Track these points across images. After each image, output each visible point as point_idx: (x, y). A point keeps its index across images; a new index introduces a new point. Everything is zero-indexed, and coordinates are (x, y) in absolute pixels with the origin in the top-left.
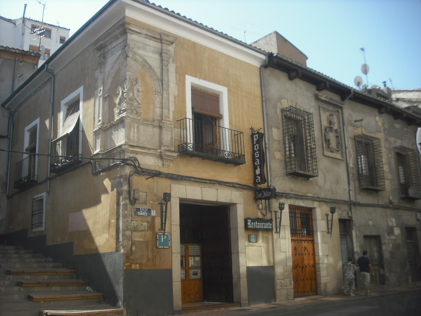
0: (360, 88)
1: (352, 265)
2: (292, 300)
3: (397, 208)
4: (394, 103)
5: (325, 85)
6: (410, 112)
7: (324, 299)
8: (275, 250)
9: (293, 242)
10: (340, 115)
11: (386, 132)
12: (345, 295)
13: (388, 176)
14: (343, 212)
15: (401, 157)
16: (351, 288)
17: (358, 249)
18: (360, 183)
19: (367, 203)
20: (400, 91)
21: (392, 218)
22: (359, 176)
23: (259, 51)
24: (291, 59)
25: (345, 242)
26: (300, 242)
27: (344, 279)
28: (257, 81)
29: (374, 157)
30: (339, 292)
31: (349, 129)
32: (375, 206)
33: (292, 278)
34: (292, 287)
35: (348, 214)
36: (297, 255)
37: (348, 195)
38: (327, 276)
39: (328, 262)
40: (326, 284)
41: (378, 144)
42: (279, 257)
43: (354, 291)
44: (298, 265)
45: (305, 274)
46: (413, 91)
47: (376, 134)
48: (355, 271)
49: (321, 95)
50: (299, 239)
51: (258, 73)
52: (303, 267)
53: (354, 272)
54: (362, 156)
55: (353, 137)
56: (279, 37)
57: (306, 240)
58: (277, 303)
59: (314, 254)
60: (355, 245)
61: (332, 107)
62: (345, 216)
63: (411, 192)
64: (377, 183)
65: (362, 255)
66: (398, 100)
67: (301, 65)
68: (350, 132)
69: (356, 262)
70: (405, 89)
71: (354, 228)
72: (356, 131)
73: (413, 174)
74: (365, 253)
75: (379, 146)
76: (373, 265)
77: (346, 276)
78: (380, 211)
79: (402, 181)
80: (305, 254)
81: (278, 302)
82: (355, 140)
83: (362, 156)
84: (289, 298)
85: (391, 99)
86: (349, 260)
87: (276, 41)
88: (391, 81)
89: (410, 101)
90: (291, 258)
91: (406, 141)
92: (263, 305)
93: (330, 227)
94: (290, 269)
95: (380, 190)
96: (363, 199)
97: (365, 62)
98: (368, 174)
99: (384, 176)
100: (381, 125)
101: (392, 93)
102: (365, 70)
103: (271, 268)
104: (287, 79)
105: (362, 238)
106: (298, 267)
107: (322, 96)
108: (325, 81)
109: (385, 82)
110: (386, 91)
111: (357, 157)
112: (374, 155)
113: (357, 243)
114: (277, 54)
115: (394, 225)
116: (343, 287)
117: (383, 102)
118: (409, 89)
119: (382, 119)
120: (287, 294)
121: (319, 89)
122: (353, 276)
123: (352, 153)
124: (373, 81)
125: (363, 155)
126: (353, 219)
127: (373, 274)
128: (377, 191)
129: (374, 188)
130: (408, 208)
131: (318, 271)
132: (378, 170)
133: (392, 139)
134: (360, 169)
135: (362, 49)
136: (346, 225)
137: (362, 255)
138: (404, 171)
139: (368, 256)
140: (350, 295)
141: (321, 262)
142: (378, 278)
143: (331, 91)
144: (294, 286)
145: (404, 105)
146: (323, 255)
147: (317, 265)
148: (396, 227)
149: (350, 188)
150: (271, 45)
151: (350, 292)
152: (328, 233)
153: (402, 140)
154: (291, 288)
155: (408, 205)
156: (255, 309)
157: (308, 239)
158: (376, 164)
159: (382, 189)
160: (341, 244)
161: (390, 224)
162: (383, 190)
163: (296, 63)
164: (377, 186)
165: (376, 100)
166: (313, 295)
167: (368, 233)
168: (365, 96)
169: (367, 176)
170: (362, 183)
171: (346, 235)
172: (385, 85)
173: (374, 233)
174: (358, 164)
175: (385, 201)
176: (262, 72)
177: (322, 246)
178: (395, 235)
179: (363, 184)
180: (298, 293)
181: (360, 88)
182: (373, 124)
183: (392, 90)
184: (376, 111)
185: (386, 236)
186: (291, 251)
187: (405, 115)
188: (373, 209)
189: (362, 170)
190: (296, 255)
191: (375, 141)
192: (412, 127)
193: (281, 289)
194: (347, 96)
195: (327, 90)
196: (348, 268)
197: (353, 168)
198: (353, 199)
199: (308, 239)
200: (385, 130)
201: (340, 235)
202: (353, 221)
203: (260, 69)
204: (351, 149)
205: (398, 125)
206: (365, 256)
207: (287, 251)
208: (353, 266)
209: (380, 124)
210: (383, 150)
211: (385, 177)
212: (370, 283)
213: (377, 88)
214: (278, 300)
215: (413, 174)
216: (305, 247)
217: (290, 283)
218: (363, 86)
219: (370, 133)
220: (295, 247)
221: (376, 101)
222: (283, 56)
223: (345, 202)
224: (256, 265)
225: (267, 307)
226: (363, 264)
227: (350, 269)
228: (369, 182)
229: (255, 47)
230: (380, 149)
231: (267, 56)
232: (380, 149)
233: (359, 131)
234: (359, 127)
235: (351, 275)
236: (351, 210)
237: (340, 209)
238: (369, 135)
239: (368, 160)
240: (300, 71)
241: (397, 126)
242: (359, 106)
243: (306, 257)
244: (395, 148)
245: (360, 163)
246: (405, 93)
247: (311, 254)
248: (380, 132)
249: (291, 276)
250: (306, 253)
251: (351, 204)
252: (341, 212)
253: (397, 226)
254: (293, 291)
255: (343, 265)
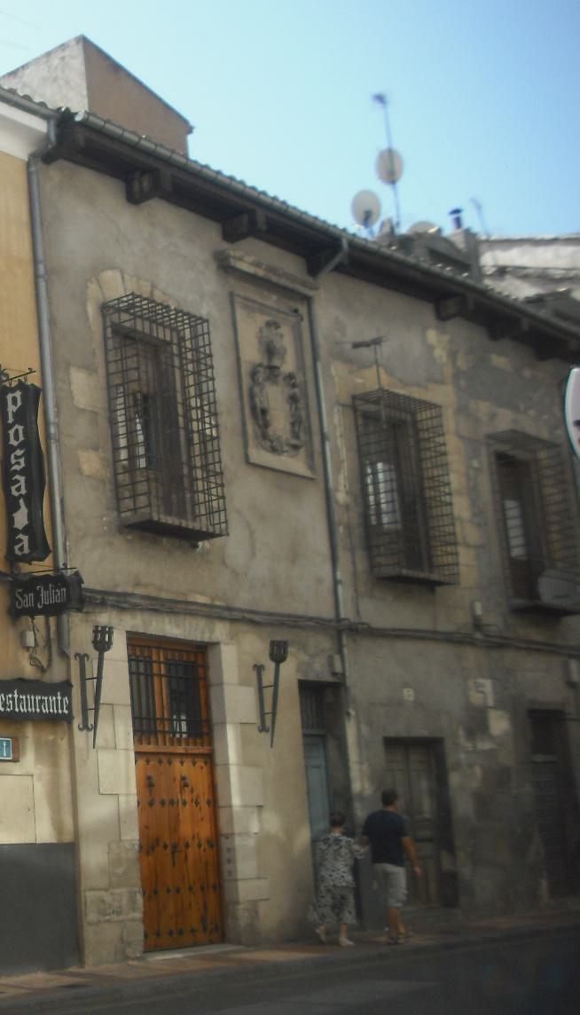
0: (371, 233)
1: (345, 839)
2: (137, 958)
3: (498, 644)
4: (488, 282)
5: (253, 222)
6: (543, 313)
7: (247, 956)
8: (80, 789)
9: (142, 762)
10: (305, 324)
11: (463, 383)
12: (321, 943)
13: (468, 532)
14: (313, 656)
15: (513, 467)
16: (340, 920)
17: (367, 785)
18: (370, 558)
19: (397, 626)
20: (508, 243)
21: (483, 677)
22: (370, 535)
23: (25, 104)
24: (134, 133)
25: (320, 761)
26: (164, 759)
27: (317, 888)
28: (19, 208)
29: (420, 469)
30: (300, 933)
31: (333, 372)
32: (422, 638)
33: (139, 883)
34: (138, 915)
35: (331, 665)
36: (157, 805)
37: (330, 601)
38: (258, 878)
39: (262, 829)
40: (254, 904)
41: (435, 422)
42: (95, 811)
43: (351, 929)
44: (157, 841)
45: (183, 871)
46: (554, 241)
47: (426, 388)
48: (356, 861)
49: (238, 254)
50: (162, 749)
51: (20, 179)
52: (175, 848)
53: (351, 862)
54: (380, 466)
55: (348, 401)
56: (94, 56)
57: (187, 755)
58: (87, 969)
59: (214, 801)
60: (356, 770)
61: (275, 297)
62: (319, 671)
63: (550, 589)
64: (430, 557)
65: (379, 807)
66: (502, 271)
67: (168, 154)
68: (337, 383)
69: (359, 830)
70: (525, 235)
71: (352, 712)
72: (359, 381)
73: (555, 528)
74: (388, 798)
75: (438, 430)
76: (417, 840)
77: (323, 879)
78: (440, 653)
79: (517, 552)
80: (184, 803)
81: (89, 967)
82: (355, 410)
83: (380, 466)
84: (129, 951)
85: (480, 269)
86: (334, 823)
87: (83, 69)
88: (479, 207)
89: (543, 276)
90: (136, 815)
91: (531, 412)
92: (38, 978)
93: (268, 709)
94: (133, 853)
95: (441, 584)
96: (382, 612)
97: (390, 141)
98: (399, 526)
99: (454, 534)
100: (445, 359)
101: (483, 247)
102: (390, 168)
103: (67, 850)
104: (123, 201)
105: (379, 748)
106: (159, 845)
107: (240, 259)
108: (251, 206)
109: (457, 211)
110: (460, 243)
111: (362, 467)
112: (420, 460)
113: (361, 763)
114: (88, 114)
115: (491, 702)
116: (313, 916)
117: (450, 281)
118: (539, 236)
119: (446, 338)
120: (121, 939)
121: (231, 236)
122: (349, 878)
123: (344, 454)
124: (418, 207)
125: (384, 461)
126: (349, 682)
127: (417, 870)
128: (431, 585)
129: (421, 575)
130: (537, 643)
131: (229, 861)
132: (434, 512)
133: (483, 408)
134: (372, 511)
135: (380, 99)
136: (323, 702)
137: (378, 806)
138: (524, 516)
139: (398, 807)
140: (336, 943)
141: (237, 828)
142: (433, 886)
143: (273, 243)
144: (145, 913)
145: (522, 291)
146: (245, 806)
147: (223, 840)
148: (495, 708)
149: (339, 575)
150: (67, 82)
151: (338, 932)
152: (263, 729)
153: (516, 409)
154: (133, 920)
155: (536, 635)
156: (12, 992)
157: (193, 749)
158: (428, 493)
159: (447, 579)
160: (306, 767)
161: (476, 698)
162: (452, 582)
163: (151, 146)
164: (431, 567)
165: (426, 273)
166: (211, 942)
167: (399, 729)
168: (388, 258)
169: (397, 532)
170: (378, 560)
171: (323, 737)
172: (458, 222)
173: (421, 731)
174: (365, 494)
175: (457, 621)
176: (34, 178)
177: (240, 775)
178: (491, 738)
179: (381, 560)
180: (158, 934)
181: (371, 233)
182: (416, 354)
183: (483, 237)
184: (426, 311)
185: (463, 741)
186: (134, 791)
187: (525, 325)
188: (418, 646)
189: (379, 513)
190: (151, 804)
191: (423, 415)
192: (550, 367)
193: (99, 922)
194: (328, 260)
195: (260, 238)
196: (331, 851)
197: (347, 507)
198: (346, 612)
199: (193, 749)
200: (457, 375)
201: (305, 736)
202: (346, 689)
203: (28, 165)
204: (340, 442)
205: (502, 360)
206: (390, 809)
207: (123, 791)
208: (349, 845)
209: (440, 354)
210: (452, 444)
211: (459, 538)
212: (407, 903)
213: (432, 231)
214: (90, 960)
215: (555, 528)
216: (183, 778)
217: (132, 901)
218: (383, 225)
219: (406, 385)
220: (149, 778)
221: (426, 276)
222: (108, 121)
223: (319, 624)
224: (14, 840)
225: (51, 984)
226: (384, 837)
227: (337, 854)
228: (403, 554)
229: (13, 91)
230: (440, 440)
231: (52, 122)
232: (440, 440)
233: (368, 381)
234: (369, 366)
235: (340, 873)
236: (340, 652)
237: (303, 648)
238: (401, 392)
239: (399, 479)
240: (167, 173)
241: (499, 361)
242: (370, 294)
243: (185, 812)
244: (493, 437)
245: (371, 489)
246: (527, 248)
247: (203, 802)
248: (441, 382)
249: (135, 876)
250: (187, 797)
251: (342, 631)
252: (305, 658)
253: (500, 705)
254: (140, 928)
255: (314, 841)
